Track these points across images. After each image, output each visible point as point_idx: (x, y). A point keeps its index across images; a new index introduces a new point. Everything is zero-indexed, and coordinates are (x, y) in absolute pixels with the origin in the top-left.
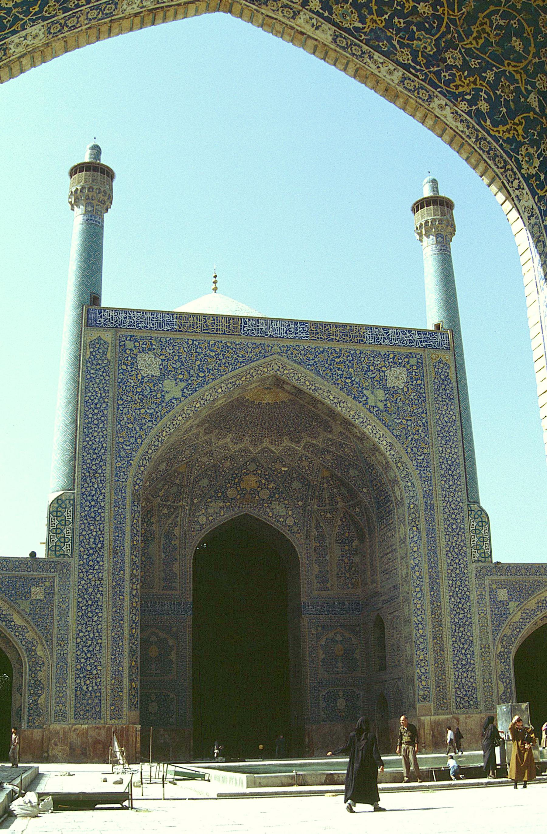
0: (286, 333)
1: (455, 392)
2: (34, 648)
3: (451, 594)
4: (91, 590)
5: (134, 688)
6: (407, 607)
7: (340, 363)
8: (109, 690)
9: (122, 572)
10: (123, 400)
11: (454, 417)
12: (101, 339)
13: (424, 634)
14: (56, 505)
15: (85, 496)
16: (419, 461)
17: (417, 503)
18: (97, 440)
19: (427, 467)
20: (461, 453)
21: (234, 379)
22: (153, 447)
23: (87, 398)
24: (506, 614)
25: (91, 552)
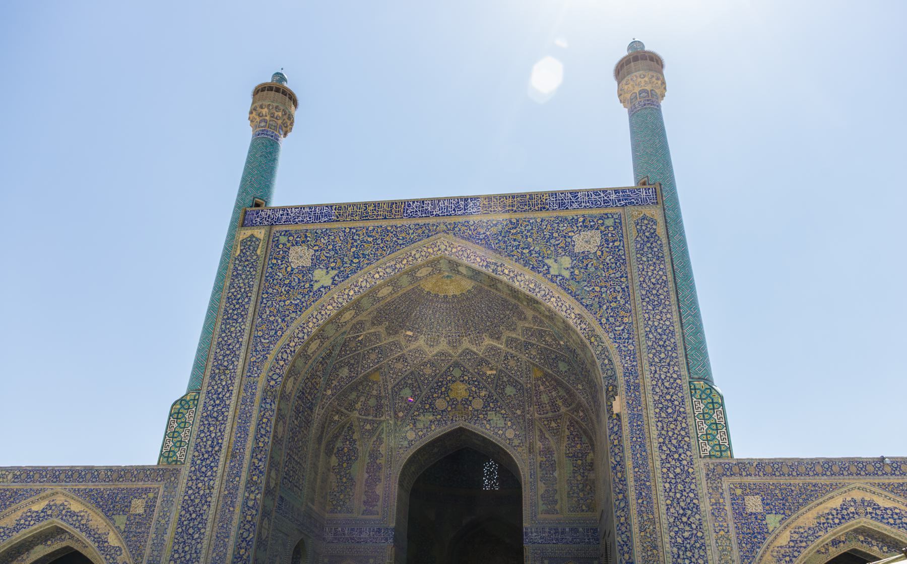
1: (666, 249)
3: (669, 502)
4: (197, 501)
7: (516, 234)
9: (237, 479)
11: (664, 278)
14: (179, 407)
16: (618, 333)
19: (629, 338)
20: (676, 318)
21: (393, 263)
22: (296, 340)
24: (763, 532)
25: (206, 456)
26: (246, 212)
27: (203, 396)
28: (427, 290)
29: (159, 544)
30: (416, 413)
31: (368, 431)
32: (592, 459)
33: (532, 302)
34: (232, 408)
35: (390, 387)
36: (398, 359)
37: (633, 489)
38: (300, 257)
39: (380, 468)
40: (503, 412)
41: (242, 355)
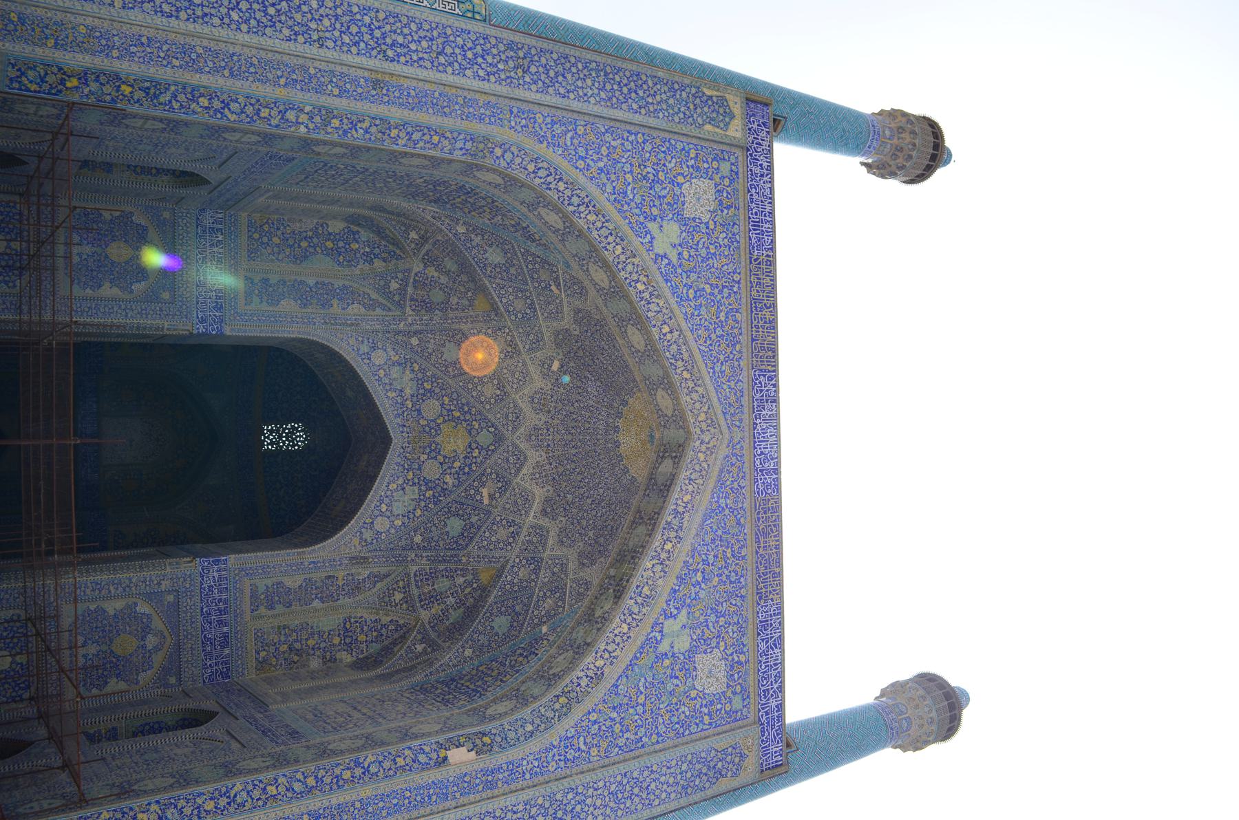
0: (762, 453)
4: (298, 17)
5: (62, 82)
6: (263, 765)
7: (725, 558)
8: (59, 17)
9: (336, 91)
11: (657, 802)
13: (203, 814)
15: (482, 41)
16: (575, 742)
17: (496, 749)
21: (686, 356)
22: (568, 193)
23: (644, 78)
25: (377, 33)
26: (766, 105)
27: (478, 27)
28: (631, 401)
30: (416, 367)
31: (387, 285)
32: (341, 660)
33: (617, 588)
34: (459, 80)
35: (463, 326)
37: (326, 803)
38: (699, 197)
39: (325, 305)
40: (418, 512)
41: (547, 99)
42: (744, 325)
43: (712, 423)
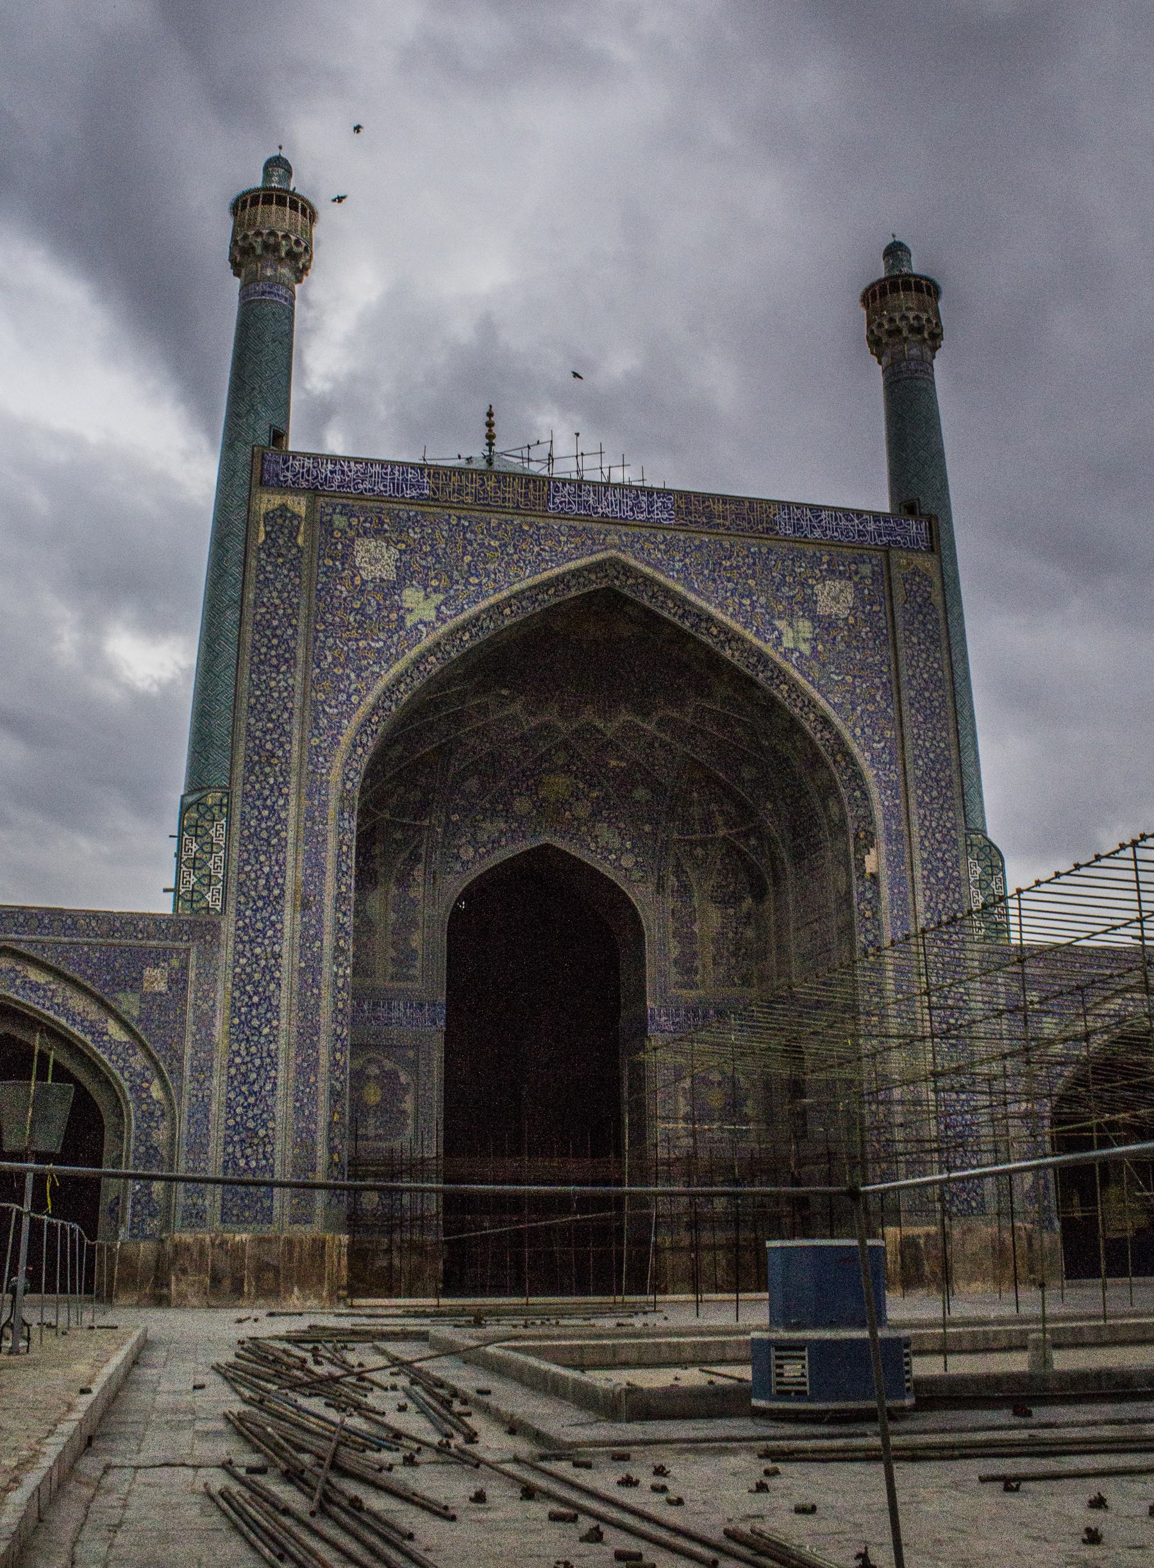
0: (632, 510)
1: (942, 626)
2: (145, 1085)
5: (336, 1165)
9: (318, 944)
10: (324, 623)
11: (940, 673)
12: (287, 509)
17: (871, 828)
18: (276, 695)
21: (534, 592)
23: (258, 617)
25: (260, 904)
27: (237, 801)
29: (206, 1042)
35: (450, 775)
36: (476, 732)
38: (375, 559)
42: (503, 516)
43: (599, 566)
